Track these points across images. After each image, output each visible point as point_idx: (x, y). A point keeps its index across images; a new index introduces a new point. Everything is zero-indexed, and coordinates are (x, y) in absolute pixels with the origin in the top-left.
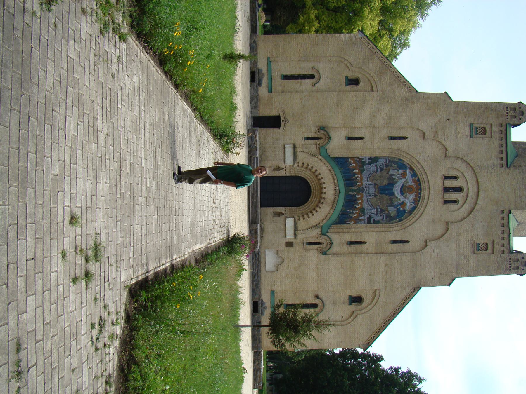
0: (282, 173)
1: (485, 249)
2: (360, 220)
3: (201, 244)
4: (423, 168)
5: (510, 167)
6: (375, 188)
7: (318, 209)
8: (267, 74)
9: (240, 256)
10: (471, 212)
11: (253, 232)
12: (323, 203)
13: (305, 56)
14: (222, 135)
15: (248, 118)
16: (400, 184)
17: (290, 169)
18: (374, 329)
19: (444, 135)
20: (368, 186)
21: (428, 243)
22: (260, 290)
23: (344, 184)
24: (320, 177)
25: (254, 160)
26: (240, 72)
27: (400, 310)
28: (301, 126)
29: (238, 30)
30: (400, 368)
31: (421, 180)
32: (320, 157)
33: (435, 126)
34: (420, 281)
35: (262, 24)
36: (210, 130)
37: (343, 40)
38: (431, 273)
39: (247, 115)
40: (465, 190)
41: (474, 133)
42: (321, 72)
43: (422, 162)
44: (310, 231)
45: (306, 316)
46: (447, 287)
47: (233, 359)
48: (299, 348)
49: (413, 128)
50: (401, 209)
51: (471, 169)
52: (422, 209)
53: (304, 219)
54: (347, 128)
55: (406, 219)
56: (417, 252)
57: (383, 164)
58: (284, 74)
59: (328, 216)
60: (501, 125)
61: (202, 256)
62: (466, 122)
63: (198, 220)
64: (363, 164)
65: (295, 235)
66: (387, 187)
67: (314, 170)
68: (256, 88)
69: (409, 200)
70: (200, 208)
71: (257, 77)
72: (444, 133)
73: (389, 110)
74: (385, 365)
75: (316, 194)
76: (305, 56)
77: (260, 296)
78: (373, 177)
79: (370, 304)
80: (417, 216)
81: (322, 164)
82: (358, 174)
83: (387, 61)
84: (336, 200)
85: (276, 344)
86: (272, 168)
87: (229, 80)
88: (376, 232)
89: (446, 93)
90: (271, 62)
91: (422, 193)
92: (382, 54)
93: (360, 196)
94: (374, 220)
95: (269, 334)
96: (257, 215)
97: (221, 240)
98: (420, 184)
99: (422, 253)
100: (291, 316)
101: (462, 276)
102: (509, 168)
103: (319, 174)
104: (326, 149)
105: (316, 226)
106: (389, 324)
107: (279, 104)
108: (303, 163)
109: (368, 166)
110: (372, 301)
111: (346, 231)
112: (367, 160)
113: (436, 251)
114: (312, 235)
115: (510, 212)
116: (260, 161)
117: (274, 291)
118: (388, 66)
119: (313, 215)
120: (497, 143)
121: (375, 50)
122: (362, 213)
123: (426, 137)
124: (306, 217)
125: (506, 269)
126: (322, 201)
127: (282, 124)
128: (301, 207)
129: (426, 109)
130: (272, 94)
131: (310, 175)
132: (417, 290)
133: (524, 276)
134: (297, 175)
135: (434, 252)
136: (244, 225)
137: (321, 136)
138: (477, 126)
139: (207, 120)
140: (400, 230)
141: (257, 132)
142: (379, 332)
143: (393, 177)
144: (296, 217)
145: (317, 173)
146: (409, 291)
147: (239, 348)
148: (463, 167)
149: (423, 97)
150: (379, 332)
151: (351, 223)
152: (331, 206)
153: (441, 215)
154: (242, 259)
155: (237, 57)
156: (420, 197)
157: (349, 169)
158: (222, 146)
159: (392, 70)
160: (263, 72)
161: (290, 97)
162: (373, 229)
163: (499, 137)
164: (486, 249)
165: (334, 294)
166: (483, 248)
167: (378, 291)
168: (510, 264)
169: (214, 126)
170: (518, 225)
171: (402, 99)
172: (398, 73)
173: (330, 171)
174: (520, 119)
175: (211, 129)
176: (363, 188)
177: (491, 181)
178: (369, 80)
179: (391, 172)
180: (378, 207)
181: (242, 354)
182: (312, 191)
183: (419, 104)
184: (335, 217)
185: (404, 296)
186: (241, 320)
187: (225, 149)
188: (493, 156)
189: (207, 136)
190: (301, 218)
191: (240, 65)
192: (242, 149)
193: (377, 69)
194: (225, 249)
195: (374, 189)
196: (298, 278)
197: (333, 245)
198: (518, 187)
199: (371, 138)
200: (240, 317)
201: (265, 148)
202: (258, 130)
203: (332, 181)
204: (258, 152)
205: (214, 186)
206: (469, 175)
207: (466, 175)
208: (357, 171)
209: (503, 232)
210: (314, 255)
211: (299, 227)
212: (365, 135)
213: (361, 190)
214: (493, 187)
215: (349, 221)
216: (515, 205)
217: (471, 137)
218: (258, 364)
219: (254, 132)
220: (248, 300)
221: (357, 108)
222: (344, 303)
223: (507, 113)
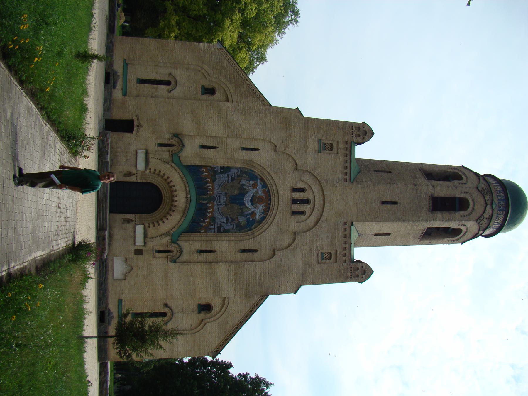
0: (133, 179)
1: (328, 259)
2: (211, 229)
3: (43, 251)
4: (273, 179)
5: (353, 182)
7: (169, 217)
8: (122, 76)
9: (86, 264)
10: (317, 223)
11: (101, 238)
12: (174, 211)
13: (163, 62)
14: (71, 136)
15: (99, 121)
17: (142, 175)
18: (223, 337)
19: (294, 149)
20: (219, 195)
21: (276, 253)
22: (107, 299)
23: (196, 192)
24: (172, 184)
25: (105, 164)
26: (94, 72)
27: (248, 317)
28: (154, 132)
29: (93, 28)
30: (249, 374)
31: (270, 191)
32: (173, 165)
33: (286, 139)
34: (268, 289)
35: (120, 24)
36: (58, 131)
37: (201, 49)
38: (278, 281)
39: (99, 117)
40: (312, 202)
41: (322, 149)
42: (177, 79)
43: (272, 174)
44: (160, 239)
45: (153, 326)
46: (293, 294)
47: (76, 372)
48: (147, 358)
49: (265, 140)
51: (318, 182)
52: (271, 219)
53: (154, 226)
54: (201, 136)
55: (256, 229)
56: (265, 261)
57: (234, 174)
58: (140, 78)
59: (179, 224)
60: (346, 143)
61: (44, 264)
62: (315, 138)
63: (40, 226)
64: (215, 173)
65: (145, 243)
67: (166, 177)
68: (110, 90)
69: (259, 210)
70: (43, 212)
71: (111, 78)
72: (294, 147)
74: (234, 372)
75: (167, 202)
76: (163, 62)
77: (107, 305)
78: (224, 187)
79: (219, 312)
80: (266, 226)
81: (174, 171)
82: (210, 182)
83: (244, 74)
84: (187, 208)
85: (122, 355)
86: (123, 173)
87: (80, 80)
88: (226, 241)
89: (297, 108)
90: (127, 64)
91: (271, 203)
92: (239, 66)
94: (224, 229)
95: (115, 345)
96: (106, 221)
97: (65, 246)
98: (270, 196)
99: (270, 262)
100: (138, 326)
101: (307, 284)
102: (352, 183)
103: (171, 181)
104: (179, 157)
105: (166, 234)
106: (238, 331)
107: (133, 108)
108: (155, 170)
110: (221, 309)
111: (197, 239)
113: (283, 260)
114: (162, 243)
115: (352, 224)
116: (111, 166)
117: (122, 300)
118: (244, 78)
119: (163, 222)
120: (342, 159)
121: (233, 61)
122: (213, 222)
123: (277, 150)
124: (156, 224)
125: (347, 278)
126: (173, 208)
127: (135, 129)
128: (151, 214)
129: (278, 122)
130: (127, 97)
131: (161, 182)
132: (265, 298)
133: (363, 283)
134: (149, 181)
135: (281, 261)
136: (91, 231)
139: (55, 120)
140: (249, 239)
141: (109, 136)
142: (227, 339)
143: (244, 187)
144: (146, 225)
145: (169, 180)
146: (257, 299)
147: (83, 360)
148: (310, 181)
149: (276, 111)
150: (227, 339)
151: (201, 232)
152: (182, 214)
153: (289, 226)
154: (88, 266)
155: (90, 56)
156: (269, 208)
158: (70, 148)
159: (248, 83)
160: (118, 74)
161: (145, 102)
162: (223, 238)
163: (344, 154)
164: (330, 259)
165: (183, 303)
166: (328, 257)
167: (226, 299)
168: (351, 273)
169: (62, 127)
170: (359, 236)
171: (256, 111)
172: (254, 86)
173: (182, 179)
174: (364, 138)
175: (58, 130)
177: (335, 194)
178: (225, 90)
179: (243, 182)
180: (229, 216)
181: (86, 366)
182: (163, 198)
184: (185, 225)
185: (252, 304)
186: (86, 331)
187: (74, 151)
188: (338, 171)
189: (54, 137)
190: (151, 225)
191: (93, 65)
192: (92, 152)
193: (233, 80)
194: (70, 257)
195: (225, 198)
196: (147, 287)
197: (183, 253)
198: (360, 201)
199: (224, 148)
200: (85, 327)
201: (116, 152)
202: (109, 134)
203: (184, 189)
204: (109, 156)
205: (60, 191)
206: (315, 188)
207: (313, 187)
208: (209, 180)
209: (346, 243)
210: (164, 264)
211: (149, 235)
212: (218, 145)
213: (212, 199)
216: (357, 217)
217: (319, 152)
218: (104, 376)
219: (106, 135)
220: (94, 309)
221: (212, 117)
222: (193, 311)
223: (352, 132)
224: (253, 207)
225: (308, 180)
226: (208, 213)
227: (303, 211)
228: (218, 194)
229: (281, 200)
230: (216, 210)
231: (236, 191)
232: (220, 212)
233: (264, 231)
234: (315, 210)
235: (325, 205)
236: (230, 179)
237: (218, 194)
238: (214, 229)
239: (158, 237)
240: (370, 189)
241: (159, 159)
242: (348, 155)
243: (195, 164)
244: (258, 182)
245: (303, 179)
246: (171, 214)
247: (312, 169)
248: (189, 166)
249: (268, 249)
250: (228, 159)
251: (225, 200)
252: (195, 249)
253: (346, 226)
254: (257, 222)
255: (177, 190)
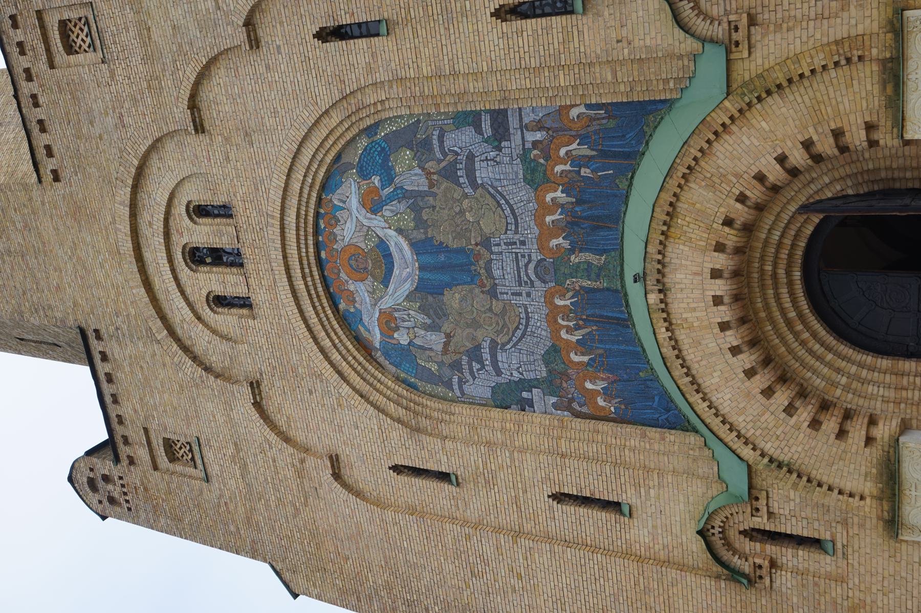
1: (71, 25)
2: (539, 126)
4: (322, 350)
6: (490, 275)
12: (728, 222)
16: (395, 291)
19: (274, 461)
20: (524, 290)
21: (241, 36)
23: (627, 305)
32: (747, 452)
33: (306, 499)
41: (196, 448)
43: (328, 371)
44: (797, 59)
49: (378, 503)
50: (376, 180)
51: (179, 332)
52: (296, 186)
53: (838, 134)
54: (627, 554)
55: (349, 136)
62: (220, 489)
64: (551, 385)
66: (446, 278)
72: (275, 466)
73: (468, 586)
81: (739, 421)
88: (455, 74)
89: (295, 596)
91: (311, 250)
93: (554, 242)
94: (479, 130)
108: (842, 434)
109: (531, 376)
112: (535, 399)
119: (781, 159)
124: (826, 146)
134: (884, 363)
137: (747, 545)
138: (191, 470)
143: (428, 321)
144: (886, 138)
148: (200, 339)
149: (359, 600)
151: (582, 109)
152: (682, 206)
156: (317, 231)
157: (611, 369)
164: (63, 25)
166: (77, 30)
176: (544, 282)
179: (435, 340)
180: (469, 190)
182: (797, 274)
183: (367, 579)
188: (127, 369)
195: (497, 273)
203: (681, 335)
207: (188, 314)
208: (576, 358)
214: (102, 266)
215: (592, 119)
216: (30, 199)
224: (380, 233)
225: (209, 342)
226: (562, 206)
227: (201, 220)
228: (529, 295)
229: (280, 269)
230: (527, 220)
231: (456, 305)
232: (508, 211)
233: (310, 130)
234: (159, 226)
235: (130, 245)
236: (486, 356)
237: (529, 295)
238: (523, 127)
239: (813, 71)
240: (28, 301)
241: (820, 485)
242: (116, 420)
243: (644, 436)
244: (378, 336)
245: (224, 346)
246: (739, 206)
247: (203, 382)
248: (672, 426)
249: (279, 47)
250: (504, 445)
251: (494, 267)
252: (598, 14)
253: (50, 167)
254: (350, 166)
255: (717, 330)
